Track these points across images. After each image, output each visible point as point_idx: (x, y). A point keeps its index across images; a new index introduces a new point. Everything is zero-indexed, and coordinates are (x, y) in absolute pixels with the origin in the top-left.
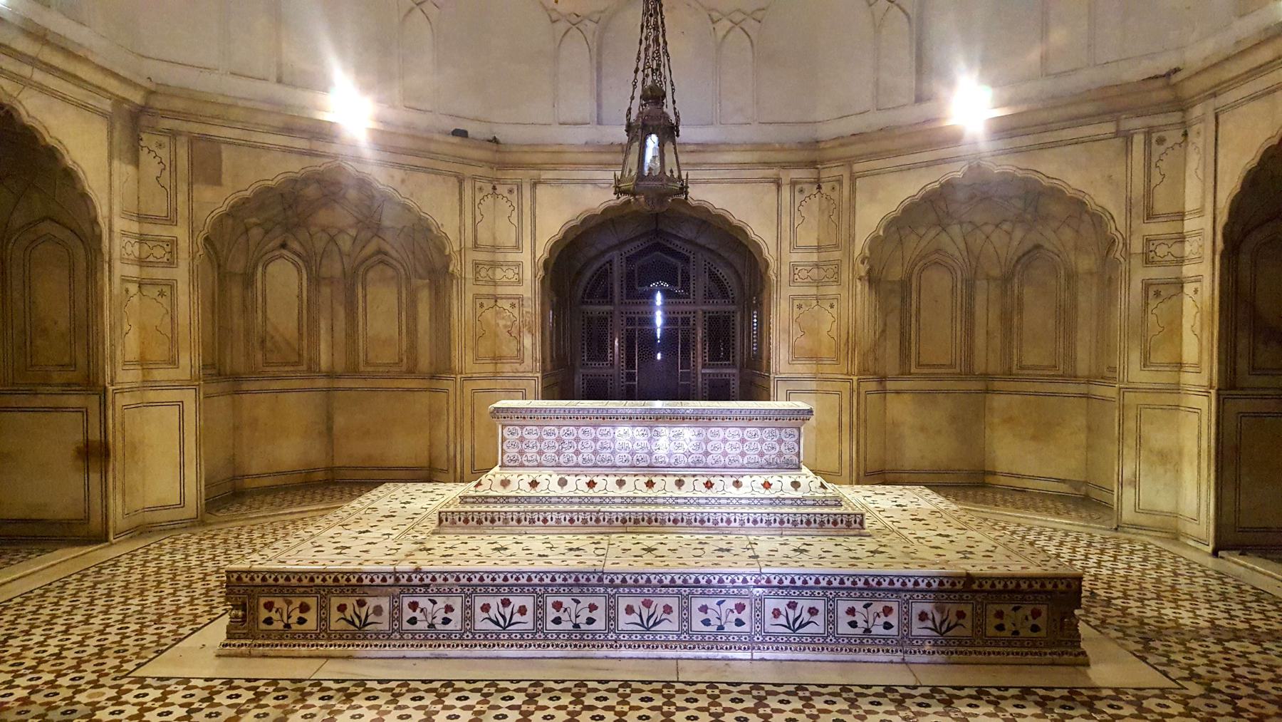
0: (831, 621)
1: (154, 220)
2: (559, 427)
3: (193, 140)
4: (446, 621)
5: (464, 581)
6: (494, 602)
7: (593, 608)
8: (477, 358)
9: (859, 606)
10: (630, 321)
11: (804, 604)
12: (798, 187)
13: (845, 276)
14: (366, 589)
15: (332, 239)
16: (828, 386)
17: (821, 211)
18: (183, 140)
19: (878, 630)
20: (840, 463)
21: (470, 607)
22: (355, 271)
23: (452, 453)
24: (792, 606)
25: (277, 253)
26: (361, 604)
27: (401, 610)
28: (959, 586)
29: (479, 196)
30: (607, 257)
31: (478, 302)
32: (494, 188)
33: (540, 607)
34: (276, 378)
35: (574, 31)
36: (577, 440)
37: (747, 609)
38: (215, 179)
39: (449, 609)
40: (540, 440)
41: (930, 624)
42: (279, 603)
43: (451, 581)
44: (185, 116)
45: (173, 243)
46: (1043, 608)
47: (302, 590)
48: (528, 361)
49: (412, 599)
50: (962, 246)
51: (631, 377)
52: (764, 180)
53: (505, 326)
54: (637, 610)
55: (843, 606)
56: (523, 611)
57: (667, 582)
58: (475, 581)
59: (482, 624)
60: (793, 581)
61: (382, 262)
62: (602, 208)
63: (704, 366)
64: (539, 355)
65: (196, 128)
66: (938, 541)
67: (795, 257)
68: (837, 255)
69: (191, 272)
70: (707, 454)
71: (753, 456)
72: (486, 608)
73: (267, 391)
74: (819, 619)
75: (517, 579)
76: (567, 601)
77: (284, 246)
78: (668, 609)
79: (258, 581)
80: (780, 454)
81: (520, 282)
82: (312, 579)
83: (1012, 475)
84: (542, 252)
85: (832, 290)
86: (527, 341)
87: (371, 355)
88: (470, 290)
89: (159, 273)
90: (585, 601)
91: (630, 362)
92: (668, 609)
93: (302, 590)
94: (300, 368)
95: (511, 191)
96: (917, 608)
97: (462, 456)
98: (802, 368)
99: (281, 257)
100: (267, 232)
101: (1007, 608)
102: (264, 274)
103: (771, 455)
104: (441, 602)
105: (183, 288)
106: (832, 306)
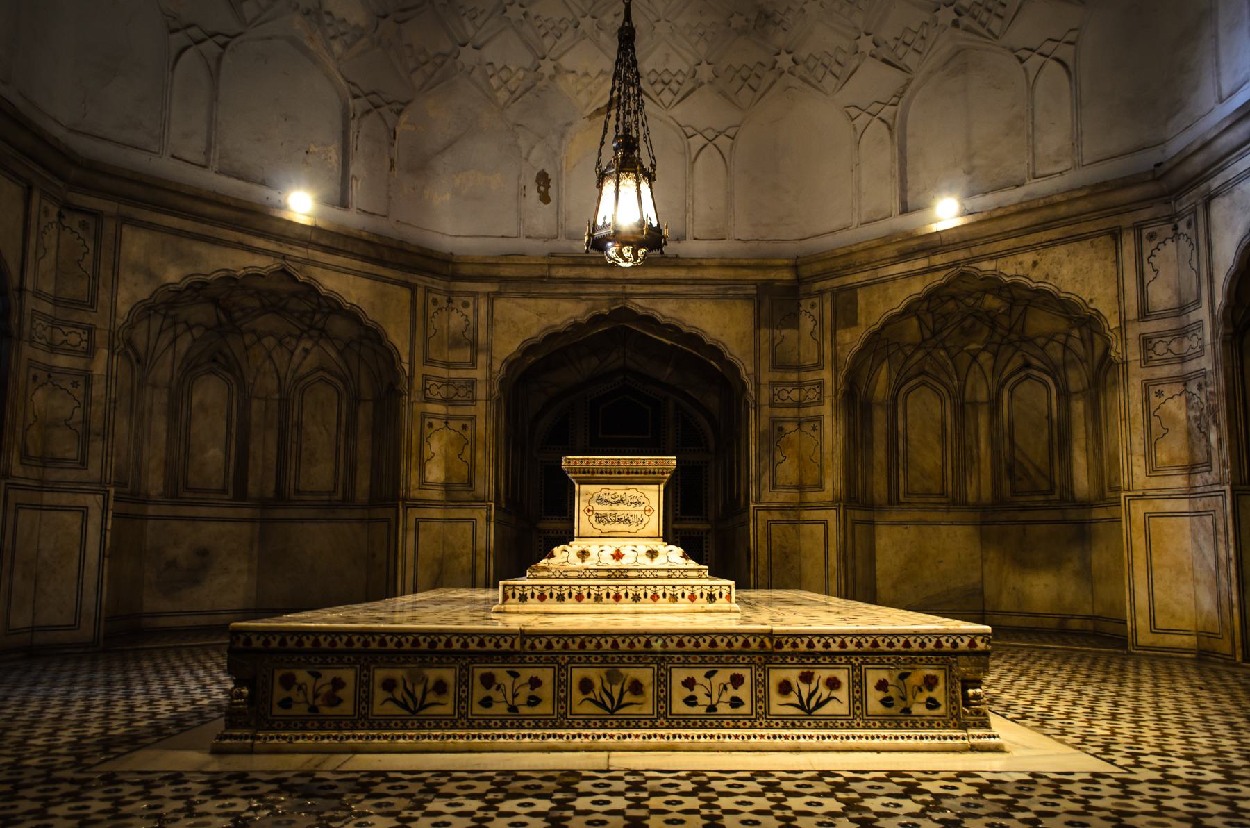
1: (808, 368)
3: (836, 293)
18: (828, 296)
25: (1022, 374)
29: (1148, 247)
34: (1024, 509)
38: (852, 322)
44: (826, 275)
45: (821, 384)
65: (836, 283)
69: (835, 406)
77: (1027, 365)
89: (811, 411)
99: (1028, 377)
100: (995, 355)
102: (1011, 397)
105: (828, 421)
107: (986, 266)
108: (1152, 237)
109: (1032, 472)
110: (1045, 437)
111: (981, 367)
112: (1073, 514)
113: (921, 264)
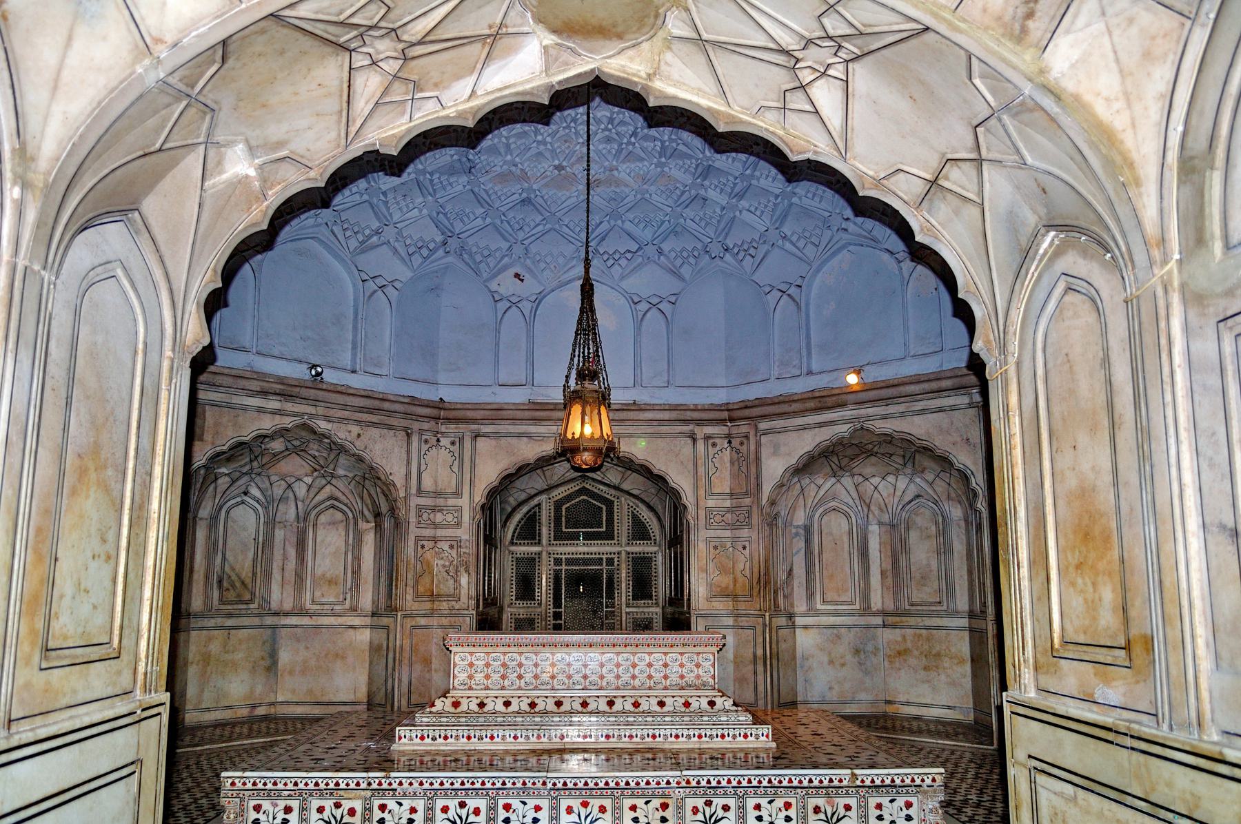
2: (504, 653)
5: (426, 786)
6: (453, 804)
7: (538, 808)
8: (417, 597)
10: (558, 562)
11: (718, 802)
12: (711, 441)
13: (755, 520)
14: (341, 793)
15: (289, 486)
16: (743, 621)
17: (732, 463)
20: (756, 695)
21: (431, 809)
22: (307, 514)
23: (390, 687)
24: (709, 803)
25: (239, 499)
26: (338, 806)
27: (370, 810)
28: (845, 783)
29: (425, 447)
30: (535, 501)
31: (420, 543)
32: (438, 440)
33: (491, 808)
35: (514, 308)
36: (520, 665)
37: (671, 808)
39: (413, 810)
40: (488, 665)
41: (822, 816)
42: (266, 805)
43: (416, 785)
46: (913, 800)
47: (287, 793)
48: (464, 599)
49: (382, 802)
50: (855, 495)
51: (557, 616)
52: (682, 434)
53: (444, 566)
54: (576, 810)
55: (751, 803)
56: (477, 812)
57: (601, 785)
58: (436, 786)
60: (709, 782)
61: (333, 507)
62: (536, 457)
63: (628, 606)
64: (474, 594)
66: (830, 749)
67: (711, 503)
68: (747, 501)
70: (634, 677)
71: (674, 678)
72: (445, 810)
73: (222, 628)
75: (473, 783)
76: (515, 803)
77: (246, 493)
78: (602, 809)
79: (249, 786)
80: (698, 677)
81: (458, 525)
82: (296, 784)
83: (909, 704)
84: (480, 498)
85: (745, 533)
86: (464, 580)
87: (318, 594)
88: (413, 531)
90: (532, 803)
91: (557, 603)
92: (602, 809)
93: (287, 793)
94: (252, 606)
95: (453, 443)
96: (812, 802)
97: (400, 690)
98: (720, 606)
101: (885, 801)
103: (690, 677)
104: (407, 804)
106: (744, 548)
107: (323, 425)
108: (426, 441)
109: (238, 584)
110: (251, 555)
111: (216, 488)
112: (269, 620)
113: (274, 404)
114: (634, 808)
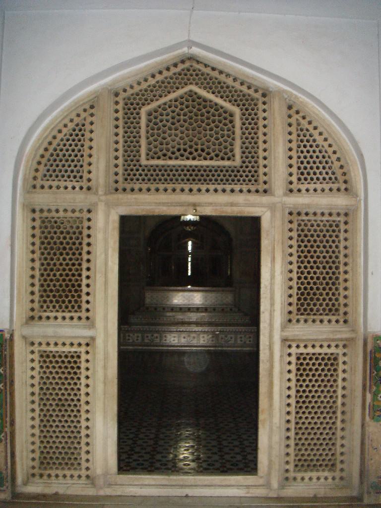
0: (236, 340)
4: (137, 340)
9: (243, 336)
11: (229, 336)
19: (248, 342)
56: (157, 337)
59: (146, 341)
74: (233, 339)
103: (225, 302)
114: (203, 337)
